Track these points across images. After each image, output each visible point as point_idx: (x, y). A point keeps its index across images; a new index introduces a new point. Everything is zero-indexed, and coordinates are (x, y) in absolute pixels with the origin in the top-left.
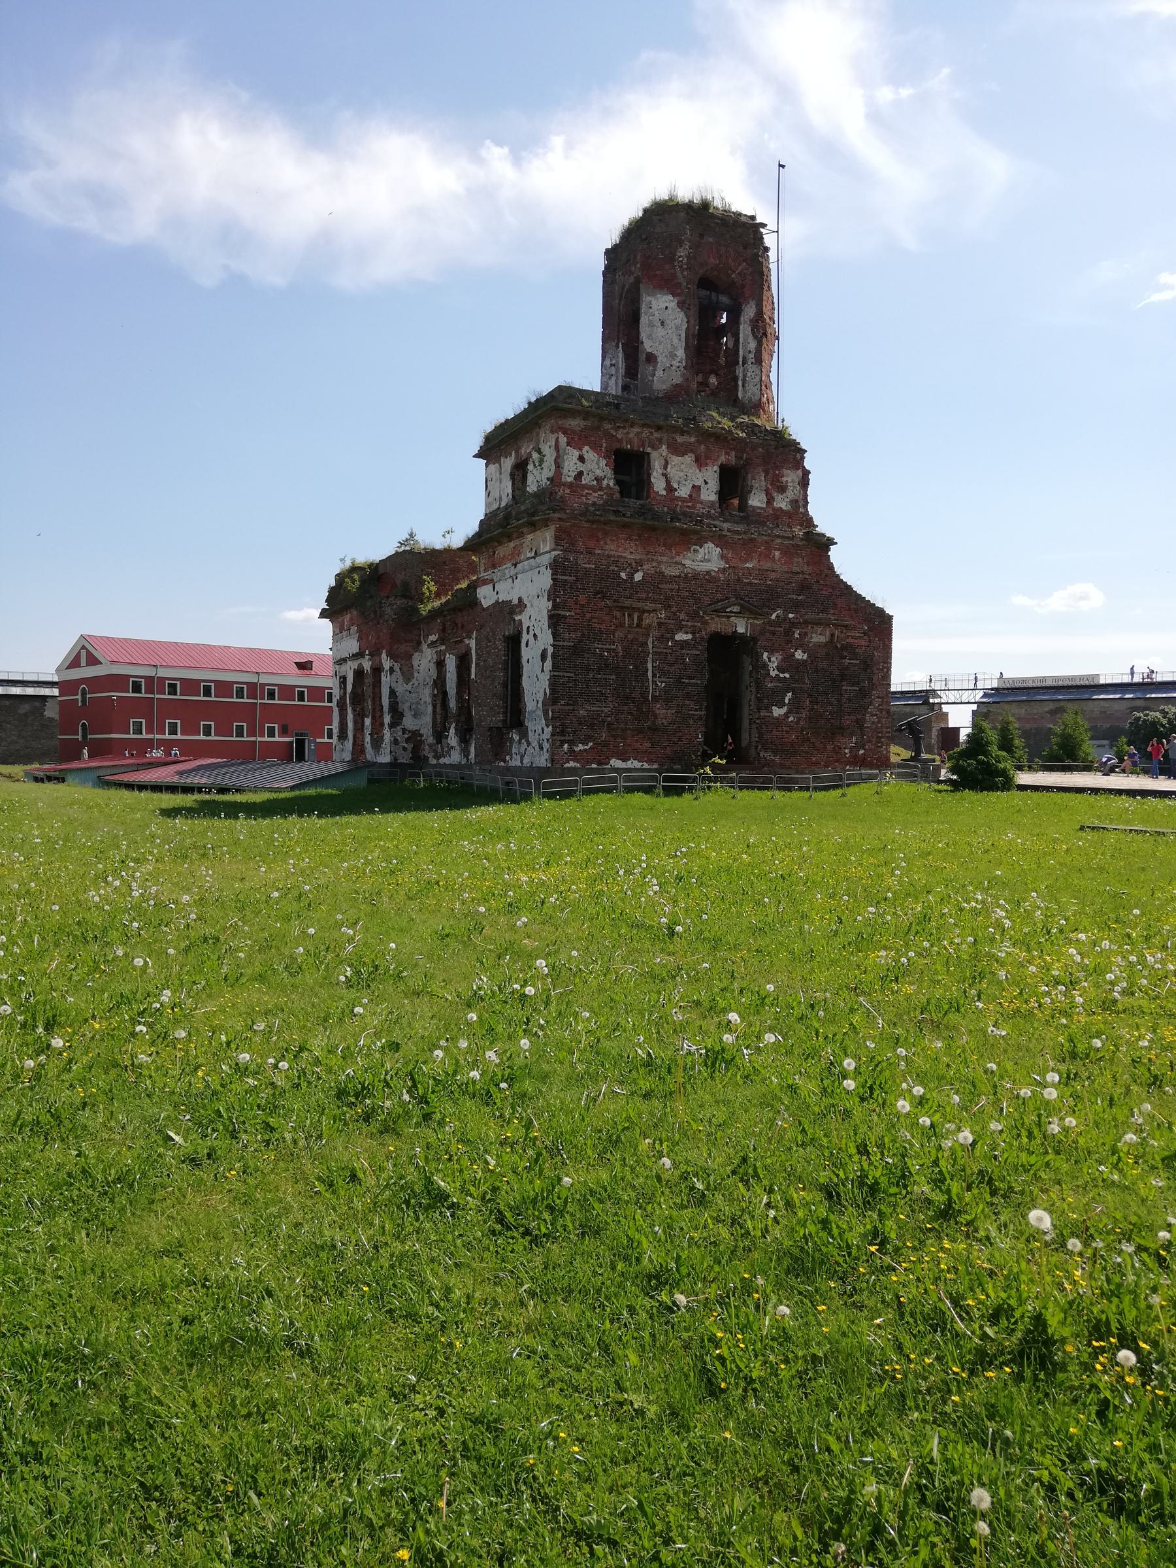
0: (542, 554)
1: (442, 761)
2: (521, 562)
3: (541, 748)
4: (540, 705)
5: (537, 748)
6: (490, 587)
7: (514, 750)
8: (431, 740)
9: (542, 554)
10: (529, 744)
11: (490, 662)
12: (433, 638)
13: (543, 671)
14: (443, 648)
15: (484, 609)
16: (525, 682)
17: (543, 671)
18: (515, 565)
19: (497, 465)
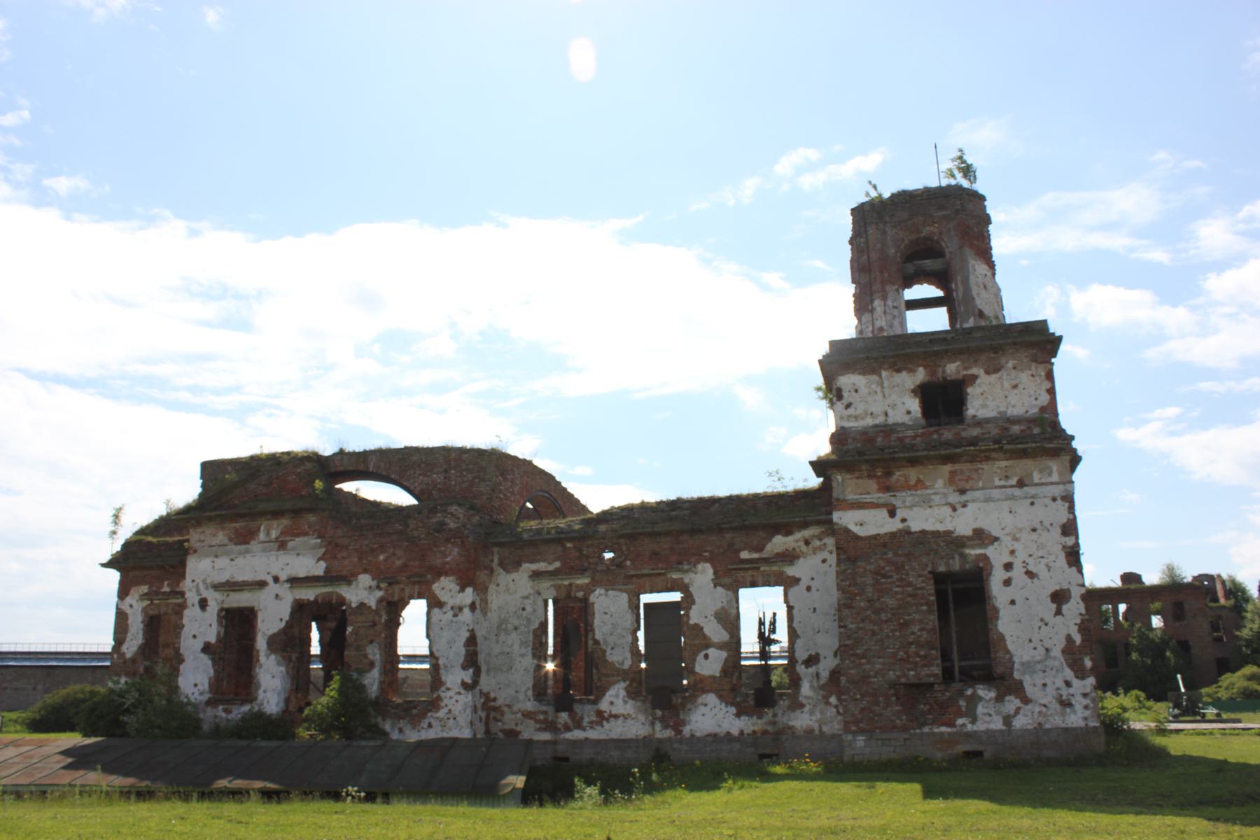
0: (1037, 485)
1: (577, 734)
2: (972, 489)
3: (1066, 704)
4: (1057, 652)
5: (1055, 706)
6: (884, 513)
7: (980, 709)
8: (530, 706)
9: (1037, 485)
10: (1026, 700)
11: (891, 602)
12: (542, 566)
13: (1059, 612)
14: (583, 581)
15: (857, 538)
16: (1006, 625)
17: (1059, 612)
18: (962, 492)
19: (875, 378)
